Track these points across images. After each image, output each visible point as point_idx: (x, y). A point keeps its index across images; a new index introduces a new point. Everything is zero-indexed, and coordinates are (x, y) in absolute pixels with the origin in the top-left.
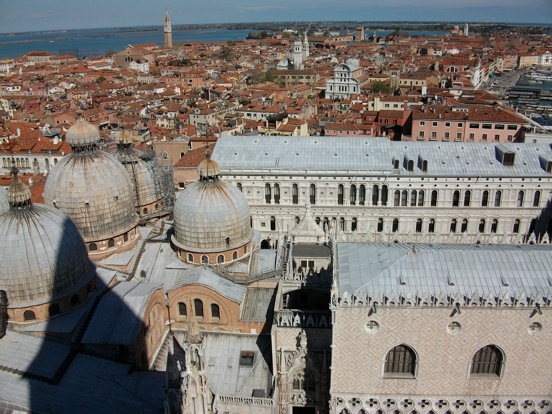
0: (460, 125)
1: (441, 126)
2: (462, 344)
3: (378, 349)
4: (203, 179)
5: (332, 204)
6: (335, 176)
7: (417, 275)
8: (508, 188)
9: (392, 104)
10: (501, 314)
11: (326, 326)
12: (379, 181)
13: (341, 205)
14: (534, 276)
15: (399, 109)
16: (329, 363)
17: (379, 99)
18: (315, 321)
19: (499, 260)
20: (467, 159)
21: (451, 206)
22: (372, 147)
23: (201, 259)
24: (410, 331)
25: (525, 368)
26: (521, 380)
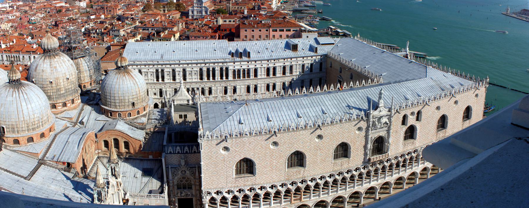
1: (256, 32)
2: (280, 153)
3: (230, 162)
5: (196, 80)
6: (197, 64)
10: (299, 133)
11: (197, 152)
13: (201, 81)
14: (315, 110)
18: (189, 150)
19: (295, 104)
21: (266, 77)
22: (218, 46)
24: (248, 150)
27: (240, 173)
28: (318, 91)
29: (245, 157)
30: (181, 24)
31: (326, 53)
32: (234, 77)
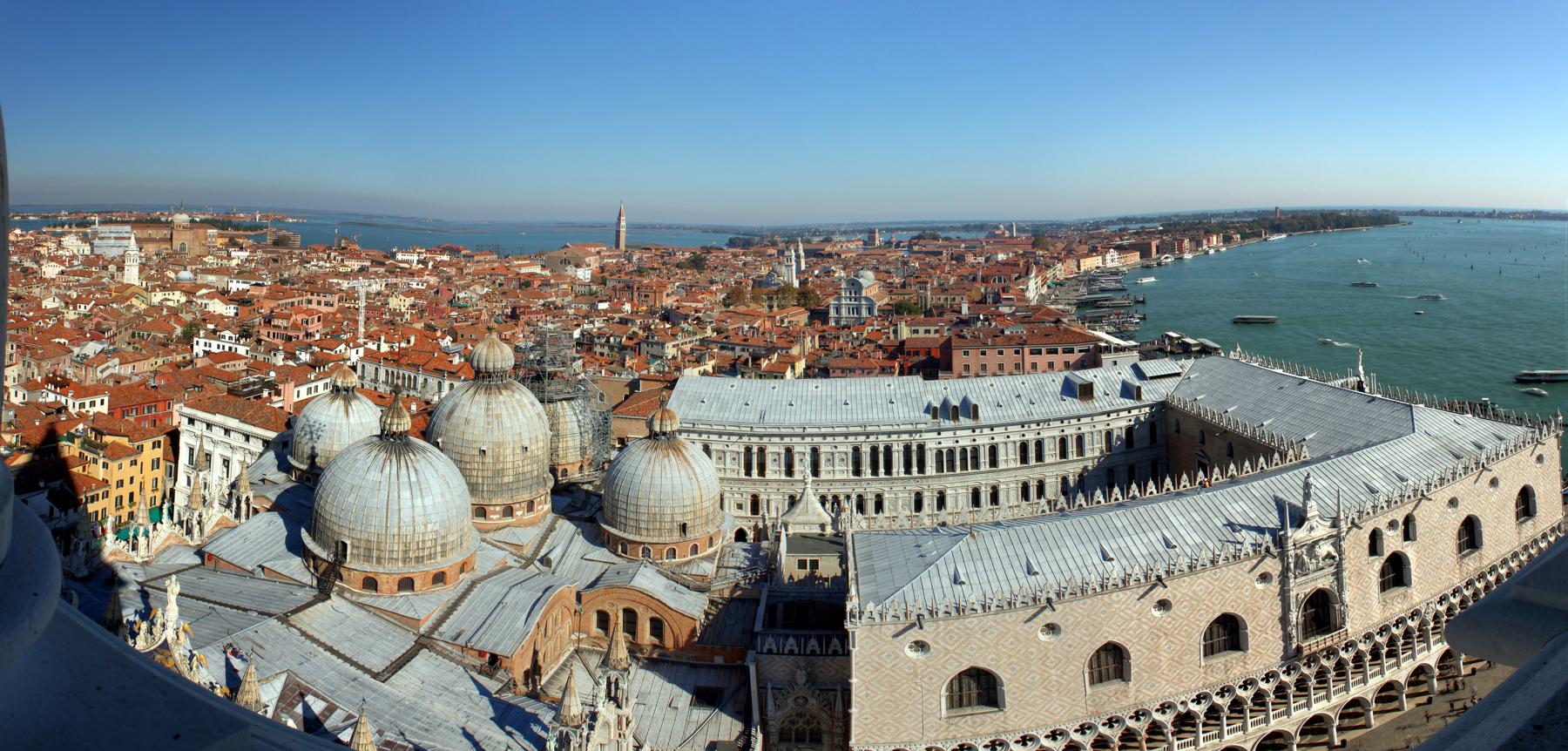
1: (992, 358)
3: (931, 678)
4: (653, 436)
5: (844, 477)
6: (846, 435)
11: (841, 652)
14: (1146, 540)
16: (847, 703)
18: (821, 647)
19: (1096, 528)
22: (898, 391)
23: (640, 552)
24: (981, 648)
27: (961, 705)
28: (1151, 493)
29: (973, 664)
30: (809, 338)
31: (1163, 399)
32: (940, 468)
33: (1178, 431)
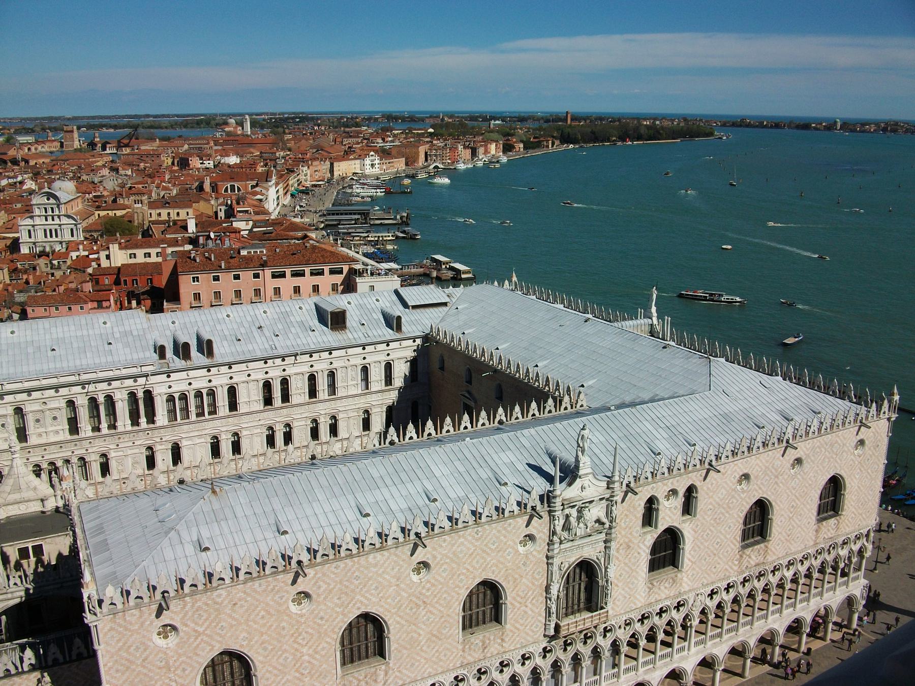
0: (256, 276)
2: (319, 625)
3: (184, 670)
6: (56, 388)
7: (226, 530)
8: (344, 365)
9: (140, 253)
10: (368, 561)
11: (86, 655)
12: (136, 384)
13: (76, 437)
14: (404, 493)
15: (154, 259)
17: (116, 246)
18: (63, 653)
19: (350, 478)
20: (275, 328)
22: (115, 329)
24: (232, 626)
25: (420, 635)
26: (418, 654)
33: (442, 368)
